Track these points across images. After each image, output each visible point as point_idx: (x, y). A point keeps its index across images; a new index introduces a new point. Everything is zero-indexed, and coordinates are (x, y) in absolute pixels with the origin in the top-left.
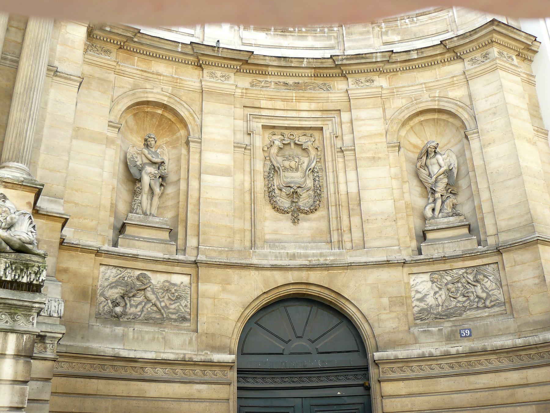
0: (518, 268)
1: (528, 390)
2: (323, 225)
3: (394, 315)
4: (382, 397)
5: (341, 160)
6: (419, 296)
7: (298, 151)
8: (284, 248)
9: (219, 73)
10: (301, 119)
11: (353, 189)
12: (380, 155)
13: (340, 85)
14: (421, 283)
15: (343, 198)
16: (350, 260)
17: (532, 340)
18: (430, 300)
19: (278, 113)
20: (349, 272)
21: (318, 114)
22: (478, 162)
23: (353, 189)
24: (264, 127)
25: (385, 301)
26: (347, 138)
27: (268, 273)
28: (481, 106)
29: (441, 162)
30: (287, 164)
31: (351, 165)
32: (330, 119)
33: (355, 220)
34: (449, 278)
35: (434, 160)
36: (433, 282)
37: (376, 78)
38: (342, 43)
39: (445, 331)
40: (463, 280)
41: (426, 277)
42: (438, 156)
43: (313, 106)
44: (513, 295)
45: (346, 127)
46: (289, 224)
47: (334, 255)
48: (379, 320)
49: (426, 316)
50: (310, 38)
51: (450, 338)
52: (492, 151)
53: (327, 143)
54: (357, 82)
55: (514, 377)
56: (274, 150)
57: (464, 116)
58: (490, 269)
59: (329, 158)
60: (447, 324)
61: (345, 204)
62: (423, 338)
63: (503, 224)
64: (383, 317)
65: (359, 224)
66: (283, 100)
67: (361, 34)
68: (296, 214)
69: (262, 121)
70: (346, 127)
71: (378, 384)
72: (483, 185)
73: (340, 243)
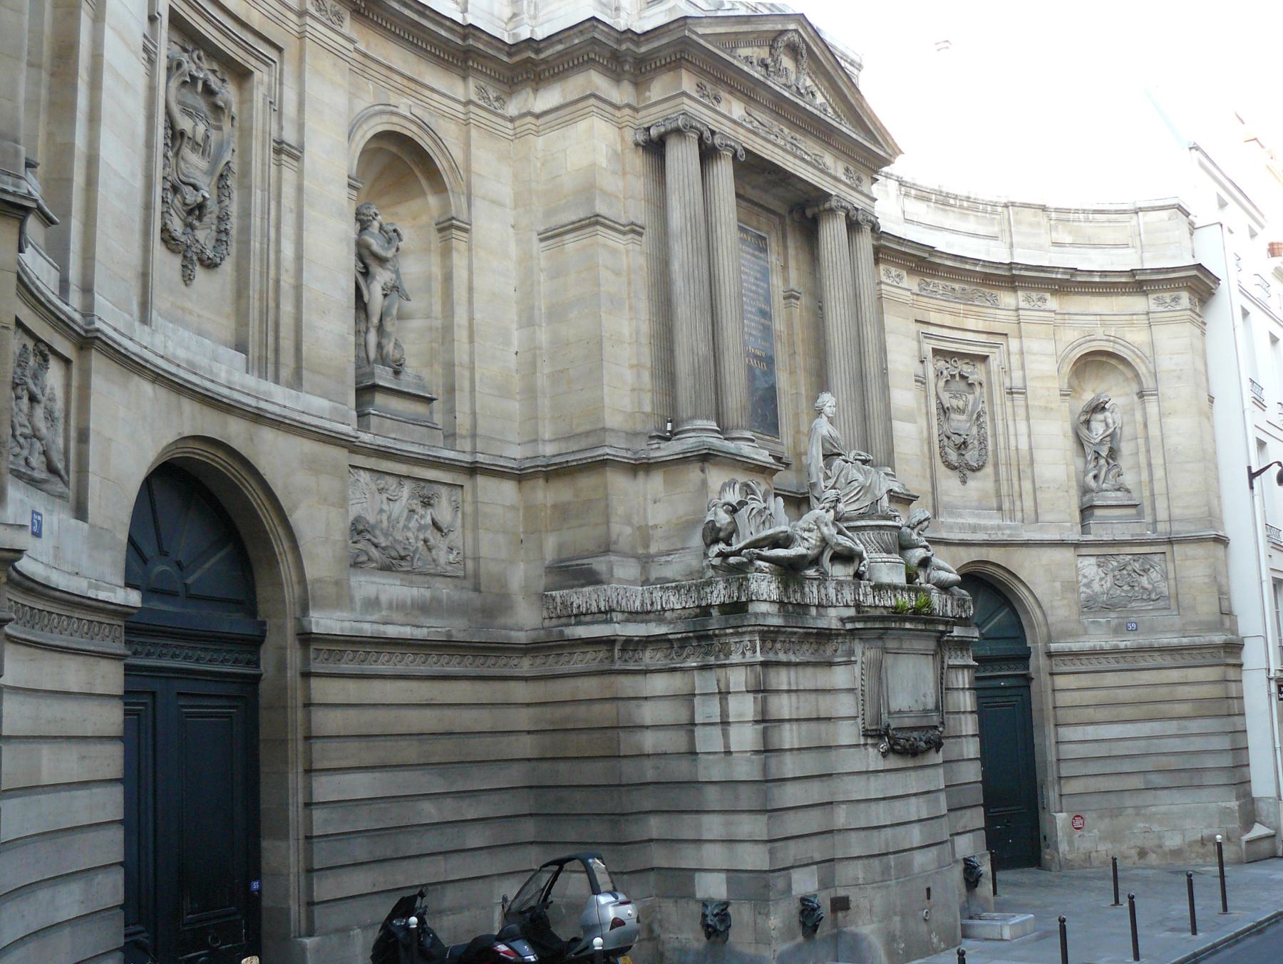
0: (1188, 563)
1: (1186, 688)
2: (989, 485)
3: (1065, 602)
4: (1054, 690)
5: (1009, 404)
6: (1085, 581)
7: (962, 385)
8: (960, 516)
9: (894, 271)
10: (969, 343)
11: (1024, 446)
12: (1053, 405)
13: (1007, 299)
14: (1089, 566)
15: (1013, 454)
16: (1026, 536)
17: (1197, 641)
18: (1096, 587)
19: (946, 332)
20: (1024, 550)
21: (983, 338)
22: (1154, 430)
23: (1024, 446)
24: (936, 352)
25: (1058, 585)
26: (1017, 374)
27: (954, 549)
28: (1166, 363)
29: (1110, 421)
30: (955, 402)
31: (1021, 412)
32: (995, 346)
33: (1027, 485)
34: (1115, 564)
35: (1100, 416)
36: (1099, 566)
37: (1048, 296)
38: (1007, 234)
39: (1114, 622)
40: (1129, 568)
41: (1093, 560)
42: (1108, 414)
43: (980, 325)
44: (1181, 591)
45: (1015, 360)
46: (958, 482)
47: (1010, 527)
48: (1052, 607)
49: (1090, 606)
50: (972, 218)
51: (1117, 631)
52: (1172, 423)
53: (995, 378)
54: (1028, 299)
55: (1175, 675)
56: (941, 383)
57: (1142, 369)
58: (1156, 558)
59: (997, 400)
60: (1113, 615)
61: (1014, 462)
62: (1092, 629)
63: (1177, 512)
64: (1055, 603)
65: (1031, 491)
66: (951, 313)
67: (1031, 225)
68: (964, 470)
69: (933, 342)
70: (1015, 360)
71: (1048, 677)
72: (1157, 461)
73: (1012, 511)
